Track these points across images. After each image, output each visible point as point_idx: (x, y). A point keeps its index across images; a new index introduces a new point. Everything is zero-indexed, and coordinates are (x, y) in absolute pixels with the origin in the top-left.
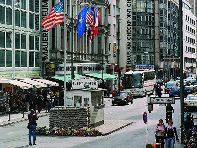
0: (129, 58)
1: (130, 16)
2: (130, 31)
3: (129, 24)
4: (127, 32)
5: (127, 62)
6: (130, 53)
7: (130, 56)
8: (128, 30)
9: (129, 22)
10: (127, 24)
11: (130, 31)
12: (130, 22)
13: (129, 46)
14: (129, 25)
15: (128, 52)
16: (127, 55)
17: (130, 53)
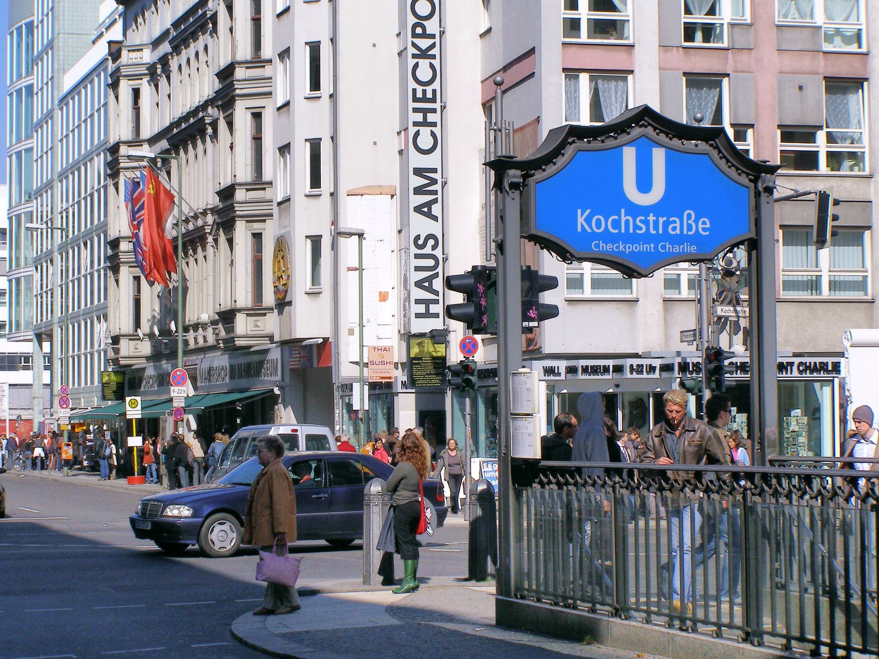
0: (430, 279)
2: (429, 95)
3: (424, 43)
4: (415, 99)
5: (418, 302)
6: (434, 247)
7: (431, 263)
8: (415, 85)
9: (425, 35)
10: (414, 45)
11: (434, 91)
12: (433, 36)
13: (434, 197)
14: (423, 54)
15: (418, 237)
16: (417, 256)
17: (431, 242)
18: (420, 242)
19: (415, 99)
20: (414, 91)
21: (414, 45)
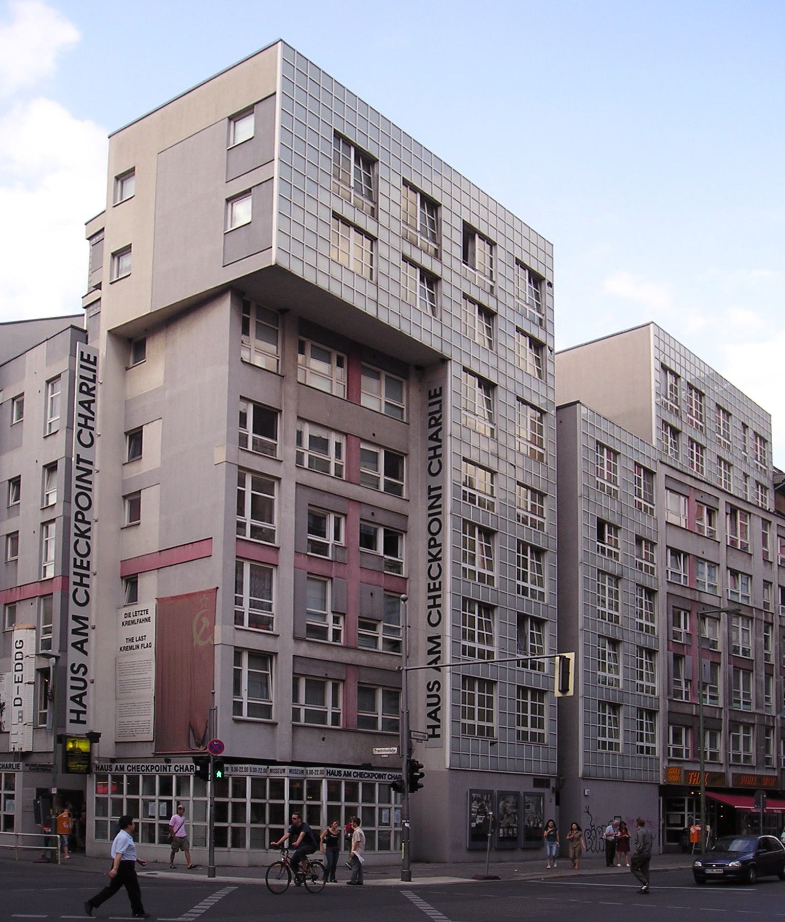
0: (81, 696)
1: (90, 490)
2: (85, 565)
3: (84, 527)
4: (75, 566)
5: (72, 711)
6: (84, 674)
7: (82, 684)
8: (77, 556)
9: (83, 521)
10: (76, 526)
11: (88, 562)
12: (89, 523)
14: (82, 534)
15: (73, 665)
16: (73, 679)
17: (82, 669)
18: (75, 669)
19: (75, 566)
20: (75, 559)
21: (76, 526)
